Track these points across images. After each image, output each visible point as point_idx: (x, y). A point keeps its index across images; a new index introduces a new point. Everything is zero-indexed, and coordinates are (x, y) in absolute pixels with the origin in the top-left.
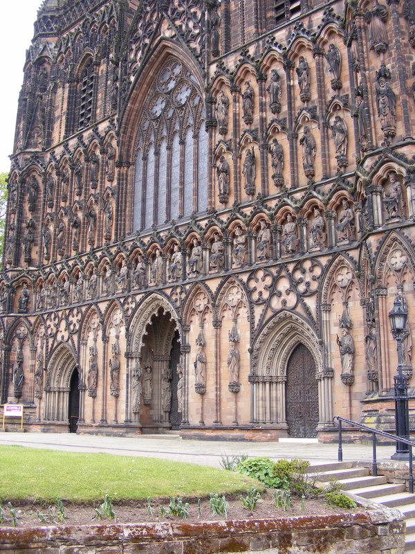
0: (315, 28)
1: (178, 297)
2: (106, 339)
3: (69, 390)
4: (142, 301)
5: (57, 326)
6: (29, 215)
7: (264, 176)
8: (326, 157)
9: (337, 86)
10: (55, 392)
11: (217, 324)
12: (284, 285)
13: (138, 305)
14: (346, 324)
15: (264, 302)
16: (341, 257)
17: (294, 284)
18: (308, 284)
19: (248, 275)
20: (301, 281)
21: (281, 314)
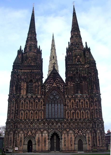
2: (42, 136)
5: (28, 132)
7: (76, 116)
8: (85, 116)
9: (87, 107)
11: (68, 136)
12: (80, 132)
13: (51, 131)
15: (77, 133)
17: (82, 132)
18: (84, 132)
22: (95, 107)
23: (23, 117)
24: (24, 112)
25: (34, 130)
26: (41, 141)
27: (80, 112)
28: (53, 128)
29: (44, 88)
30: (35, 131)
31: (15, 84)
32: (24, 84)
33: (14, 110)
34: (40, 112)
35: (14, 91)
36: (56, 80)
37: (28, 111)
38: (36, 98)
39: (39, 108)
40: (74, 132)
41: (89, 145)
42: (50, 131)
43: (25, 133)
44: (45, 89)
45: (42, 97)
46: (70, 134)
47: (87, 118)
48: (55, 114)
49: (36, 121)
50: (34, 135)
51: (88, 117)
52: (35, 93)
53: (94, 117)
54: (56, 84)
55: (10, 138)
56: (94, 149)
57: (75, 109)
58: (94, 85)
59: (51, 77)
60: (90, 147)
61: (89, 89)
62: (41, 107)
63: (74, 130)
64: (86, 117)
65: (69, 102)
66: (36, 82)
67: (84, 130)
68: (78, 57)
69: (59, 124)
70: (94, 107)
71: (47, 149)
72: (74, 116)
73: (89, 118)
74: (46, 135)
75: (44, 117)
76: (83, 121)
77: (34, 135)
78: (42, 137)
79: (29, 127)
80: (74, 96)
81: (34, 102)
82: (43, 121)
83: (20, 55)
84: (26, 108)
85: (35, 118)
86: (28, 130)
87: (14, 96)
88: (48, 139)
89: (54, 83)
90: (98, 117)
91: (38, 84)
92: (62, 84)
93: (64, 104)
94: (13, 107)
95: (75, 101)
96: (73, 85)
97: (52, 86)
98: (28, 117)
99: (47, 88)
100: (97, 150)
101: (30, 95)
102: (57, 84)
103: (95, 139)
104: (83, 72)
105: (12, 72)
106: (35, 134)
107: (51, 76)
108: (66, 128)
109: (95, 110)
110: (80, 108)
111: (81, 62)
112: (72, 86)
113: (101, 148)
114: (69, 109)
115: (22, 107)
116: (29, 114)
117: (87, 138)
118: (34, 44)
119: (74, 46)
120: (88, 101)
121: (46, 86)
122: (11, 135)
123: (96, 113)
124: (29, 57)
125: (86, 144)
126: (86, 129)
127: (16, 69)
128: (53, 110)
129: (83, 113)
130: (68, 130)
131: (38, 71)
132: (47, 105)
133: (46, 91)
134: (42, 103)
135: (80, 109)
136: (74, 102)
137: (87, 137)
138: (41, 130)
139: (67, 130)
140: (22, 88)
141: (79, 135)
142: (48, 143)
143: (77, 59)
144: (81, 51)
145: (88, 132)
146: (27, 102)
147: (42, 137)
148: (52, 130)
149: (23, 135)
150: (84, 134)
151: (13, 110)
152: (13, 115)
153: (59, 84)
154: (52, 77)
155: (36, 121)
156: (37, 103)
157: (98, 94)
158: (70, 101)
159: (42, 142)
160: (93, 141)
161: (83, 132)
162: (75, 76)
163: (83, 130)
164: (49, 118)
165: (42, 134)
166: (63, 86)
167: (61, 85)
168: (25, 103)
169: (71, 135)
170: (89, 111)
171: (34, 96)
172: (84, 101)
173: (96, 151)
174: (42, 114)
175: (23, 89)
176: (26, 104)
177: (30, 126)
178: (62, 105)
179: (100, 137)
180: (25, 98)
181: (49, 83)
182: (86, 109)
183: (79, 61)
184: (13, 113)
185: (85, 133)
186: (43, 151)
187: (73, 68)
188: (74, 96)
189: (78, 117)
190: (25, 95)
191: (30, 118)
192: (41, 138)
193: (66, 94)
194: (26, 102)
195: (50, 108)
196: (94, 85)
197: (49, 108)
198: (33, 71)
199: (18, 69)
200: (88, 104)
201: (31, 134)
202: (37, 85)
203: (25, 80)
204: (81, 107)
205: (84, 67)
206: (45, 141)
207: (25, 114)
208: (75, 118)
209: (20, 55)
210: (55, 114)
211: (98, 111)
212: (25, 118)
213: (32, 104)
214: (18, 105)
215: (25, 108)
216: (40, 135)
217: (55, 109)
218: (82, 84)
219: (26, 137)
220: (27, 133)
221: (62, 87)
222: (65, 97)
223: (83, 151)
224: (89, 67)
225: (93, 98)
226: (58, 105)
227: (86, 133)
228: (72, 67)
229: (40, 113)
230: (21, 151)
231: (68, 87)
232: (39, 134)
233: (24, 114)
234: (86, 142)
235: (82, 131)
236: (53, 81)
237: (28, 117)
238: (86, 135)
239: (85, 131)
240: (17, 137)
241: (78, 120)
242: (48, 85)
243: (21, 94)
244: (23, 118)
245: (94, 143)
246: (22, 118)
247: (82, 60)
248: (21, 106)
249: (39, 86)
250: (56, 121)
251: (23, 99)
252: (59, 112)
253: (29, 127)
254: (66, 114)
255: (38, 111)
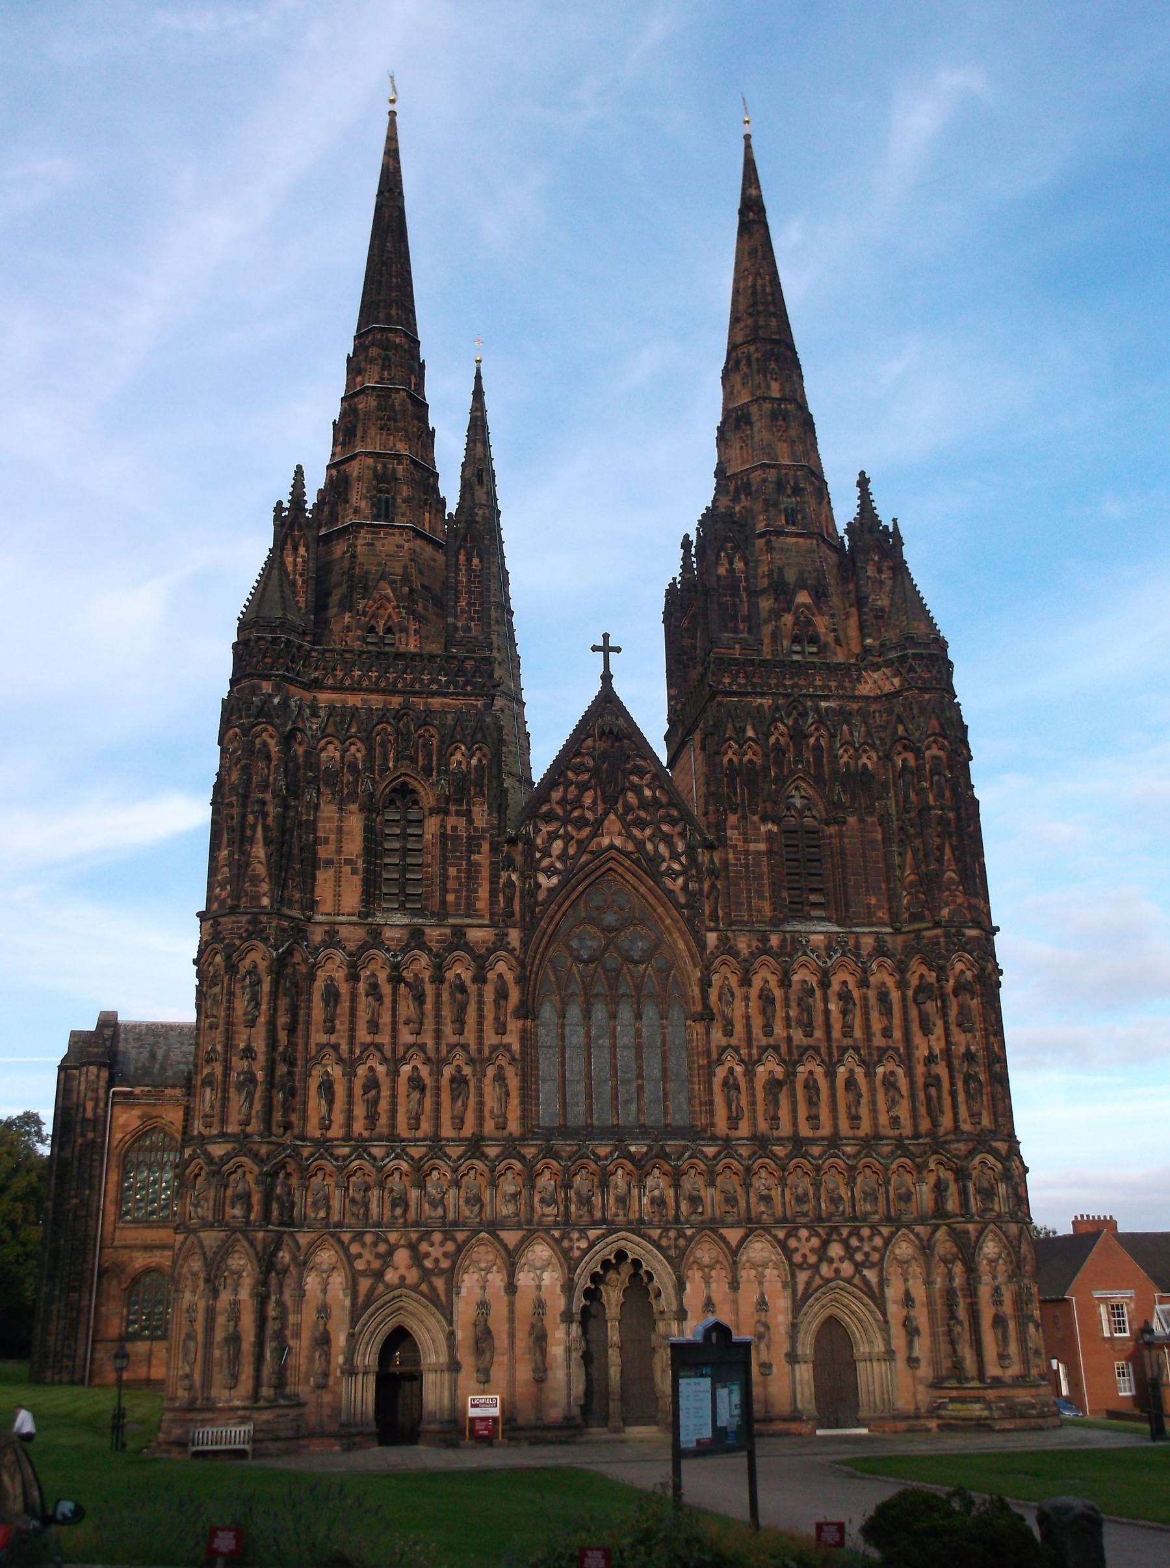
0: (864, 953)
1: (672, 1243)
2: (511, 1288)
3: (377, 1369)
4: (598, 1238)
5: (387, 1258)
6: (283, 1036)
7: (794, 1111)
8: (874, 1111)
9: (887, 1033)
10: (357, 1374)
11: (734, 1285)
12: (835, 1250)
13: (592, 1245)
14: (908, 1300)
15: (811, 1266)
16: (904, 1230)
17: (850, 1252)
18: (867, 1254)
19: (785, 1231)
20: (858, 1249)
21: (832, 1284)
22: (960, 1039)
23: (338, 1117)
24: (350, 1074)
25: (437, 1237)
26: (504, 1336)
27: (831, 1075)
28: (603, 1221)
29: (519, 859)
30: (450, 1247)
31: (265, 815)
32: (341, 820)
33: (261, 1058)
34: (491, 1071)
35: (255, 880)
36: (623, 791)
37: (385, 1060)
38: (452, 948)
39: (480, 1039)
40: (788, 1252)
41: (912, 1362)
42: (584, 1244)
43: (360, 1265)
44: (531, 868)
45: (502, 937)
46: (746, 1275)
47: (889, 1132)
48: (615, 1097)
49: (455, 1152)
50: (439, 1283)
51: (895, 1121)
52: (444, 902)
53: (947, 1121)
54: (627, 826)
55: (221, 1320)
56: (953, 1400)
57: (790, 1053)
58: (947, 850)
59: (578, 770)
60: (921, 1388)
61: (901, 880)
62: (501, 1030)
63: (781, 1234)
64: (883, 1119)
65: (738, 992)
66: (453, 808)
67: (866, 1232)
68: (803, 598)
69: (657, 1183)
70: (948, 1042)
71: (554, 1404)
72: (784, 1112)
73: (907, 1131)
74: (551, 1279)
75: (523, 1117)
76: (855, 1156)
77: (439, 1283)
78: (511, 1305)
79: (398, 1211)
80: (774, 940)
81: (438, 979)
82: (522, 1158)
83: (302, 550)
84: (363, 1035)
85: (447, 1131)
86: (386, 1241)
87: (254, 921)
88: (567, 1317)
89: (606, 814)
90: (986, 1121)
91: (470, 821)
92: (678, 829)
93: (698, 1008)
94: (251, 1024)
95: (785, 983)
96: (762, 847)
97: (593, 846)
98: (383, 1120)
99: (545, 863)
100: (986, 1413)
101: (399, 919)
102: (636, 832)
103: (962, 1312)
104: (847, 737)
105: (230, 709)
106: (451, 1276)
107: (578, 754)
108: (718, 1213)
109: (956, 1062)
110: (829, 1047)
111: (823, 649)
112: (759, 853)
113: (1023, 1396)
114: (736, 1049)
115: (331, 1031)
116: (393, 1089)
117: (895, 1310)
118: (413, 462)
119: (758, 507)
120: (890, 982)
121: (539, 841)
122: (236, 1291)
123: (967, 1092)
124: (383, 577)
125: (890, 1355)
126: (885, 1231)
127: (266, 677)
128: (600, 1059)
129: (850, 1083)
130: (733, 1235)
131: (460, 702)
132: (547, 1012)
133: (539, 886)
134: (502, 994)
135: (830, 1055)
136: (778, 993)
137: (893, 1293)
138: (504, 1235)
139: (723, 1239)
140: (323, 853)
141: (828, 1281)
142: (568, 1350)
143: (788, 619)
144: (824, 547)
145: (904, 1248)
146: (374, 990)
147: (511, 1305)
148: (603, 1237)
149: (338, 1280)
150: (871, 1275)
151: (248, 1053)
152: (251, 1106)
153: (648, 832)
154: (589, 762)
155: (455, 1152)
156: (463, 989)
157: (978, 925)
158: (746, 982)
159: (512, 1344)
160: (950, 1332)
161: (859, 1257)
162: (779, 765)
163: (855, 1232)
164: (565, 1131)
165: (511, 1275)
166: (680, 846)
167: (668, 840)
168: (354, 996)
169: (761, 1283)
170: (900, 1071)
171: (434, 934)
172: (863, 983)
173: (981, 1426)
174: (508, 1095)
175: (329, 862)
176: (364, 1003)
177: (401, 1201)
178: (676, 1014)
179: (1007, 1297)
180: (351, 946)
181: (565, 821)
182: (883, 1051)
183: (805, 635)
184: (251, 1079)
185: (872, 1266)
186: (521, 1428)
187: (762, 695)
188: (774, 940)
189: (813, 1119)
190: (354, 919)
191: (403, 1130)
192: (499, 1310)
193: (714, 917)
194: (362, 987)
195: (576, 1038)
196: (947, 850)
197: (562, 1037)
198: (419, 703)
199: (291, 681)
200: (891, 1008)
201: (413, 1276)
202: (454, 829)
203: (348, 777)
204: (836, 1033)
205: (854, 689)
206: (540, 1339)
207: (358, 1090)
208: (785, 1129)
209: (302, 550)
210: (615, 1097)
211: (982, 1077)
212: (358, 1127)
213: (420, 999)
214: (294, 1010)
215: (352, 1038)
216: (497, 1279)
217: (614, 1046)
218: (840, 835)
219: (366, 1306)
220: (376, 1264)
221: (675, 856)
222: (702, 945)
223: (859, 1423)
224: (897, 694)
225: (942, 957)
226: (638, 1016)
227: (882, 1258)
228: (754, 686)
229: (488, 1080)
230: (323, 1435)
231: (725, 863)
232: (488, 1270)
233: (350, 1095)
234: (887, 1341)
235: (854, 1242)
236: (594, 803)
237: (383, 1120)
238: (882, 1282)
239: (875, 1249)
240: (287, 1297)
241: (816, 1150)
242: (553, 836)
243: (312, 905)
244: (336, 1132)
245: (959, 1348)
246: (328, 1128)
247: (834, 630)
248: (318, 1011)
249: (473, 845)
250: (630, 1157)
251: (339, 956)
252: (653, 1069)
253: (398, 1211)
254: (710, 1091)
255: (471, 1061)
